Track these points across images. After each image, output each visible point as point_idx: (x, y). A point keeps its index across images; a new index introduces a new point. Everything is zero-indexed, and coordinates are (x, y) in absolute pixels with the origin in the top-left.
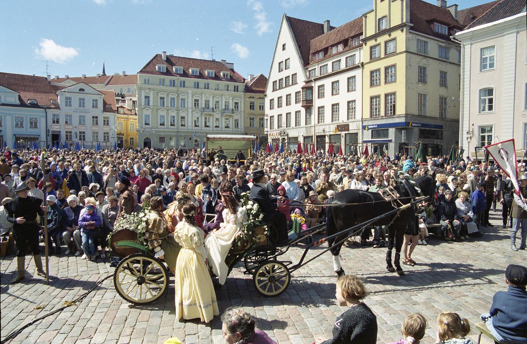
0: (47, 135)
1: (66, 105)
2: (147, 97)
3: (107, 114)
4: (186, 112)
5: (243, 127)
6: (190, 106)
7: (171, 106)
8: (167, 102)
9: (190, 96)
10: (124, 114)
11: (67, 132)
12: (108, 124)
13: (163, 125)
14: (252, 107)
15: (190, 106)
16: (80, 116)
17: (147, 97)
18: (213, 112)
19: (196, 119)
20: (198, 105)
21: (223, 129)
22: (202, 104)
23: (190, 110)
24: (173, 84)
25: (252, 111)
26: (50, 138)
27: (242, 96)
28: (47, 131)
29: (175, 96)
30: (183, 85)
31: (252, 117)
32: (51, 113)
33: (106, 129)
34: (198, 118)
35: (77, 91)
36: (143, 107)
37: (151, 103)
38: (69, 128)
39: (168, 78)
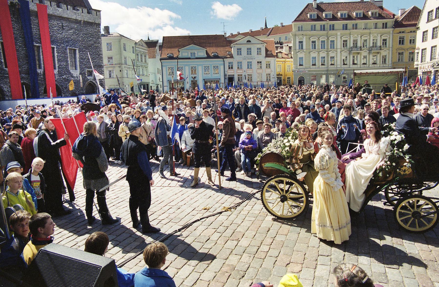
0: (225, 78)
1: (238, 54)
2: (301, 42)
3: (268, 59)
4: (335, 52)
5: (390, 62)
6: (339, 46)
7: (322, 48)
8: (318, 45)
9: (339, 37)
10: (283, 58)
11: (238, 75)
12: (269, 67)
13: (315, 65)
14: (402, 42)
15: (339, 46)
16: (248, 62)
17: (301, 42)
18: (361, 50)
19: (344, 58)
20: (346, 46)
21: (371, 66)
22: (350, 44)
23: (339, 51)
24: (323, 28)
25: (401, 46)
26: (227, 81)
27: (391, 32)
28: (225, 75)
29: (325, 39)
30: (332, 28)
31: (401, 52)
32: (227, 61)
33: (268, 71)
34: (346, 57)
35: (246, 42)
36: (297, 51)
37: (304, 47)
38: (240, 72)
39: (318, 24)
